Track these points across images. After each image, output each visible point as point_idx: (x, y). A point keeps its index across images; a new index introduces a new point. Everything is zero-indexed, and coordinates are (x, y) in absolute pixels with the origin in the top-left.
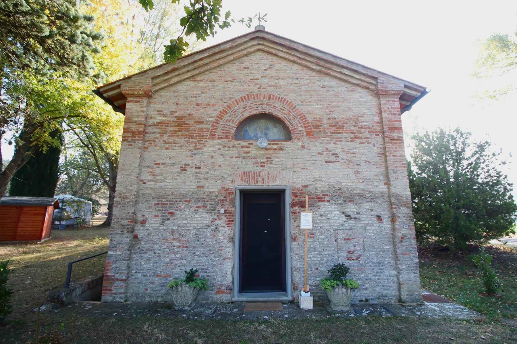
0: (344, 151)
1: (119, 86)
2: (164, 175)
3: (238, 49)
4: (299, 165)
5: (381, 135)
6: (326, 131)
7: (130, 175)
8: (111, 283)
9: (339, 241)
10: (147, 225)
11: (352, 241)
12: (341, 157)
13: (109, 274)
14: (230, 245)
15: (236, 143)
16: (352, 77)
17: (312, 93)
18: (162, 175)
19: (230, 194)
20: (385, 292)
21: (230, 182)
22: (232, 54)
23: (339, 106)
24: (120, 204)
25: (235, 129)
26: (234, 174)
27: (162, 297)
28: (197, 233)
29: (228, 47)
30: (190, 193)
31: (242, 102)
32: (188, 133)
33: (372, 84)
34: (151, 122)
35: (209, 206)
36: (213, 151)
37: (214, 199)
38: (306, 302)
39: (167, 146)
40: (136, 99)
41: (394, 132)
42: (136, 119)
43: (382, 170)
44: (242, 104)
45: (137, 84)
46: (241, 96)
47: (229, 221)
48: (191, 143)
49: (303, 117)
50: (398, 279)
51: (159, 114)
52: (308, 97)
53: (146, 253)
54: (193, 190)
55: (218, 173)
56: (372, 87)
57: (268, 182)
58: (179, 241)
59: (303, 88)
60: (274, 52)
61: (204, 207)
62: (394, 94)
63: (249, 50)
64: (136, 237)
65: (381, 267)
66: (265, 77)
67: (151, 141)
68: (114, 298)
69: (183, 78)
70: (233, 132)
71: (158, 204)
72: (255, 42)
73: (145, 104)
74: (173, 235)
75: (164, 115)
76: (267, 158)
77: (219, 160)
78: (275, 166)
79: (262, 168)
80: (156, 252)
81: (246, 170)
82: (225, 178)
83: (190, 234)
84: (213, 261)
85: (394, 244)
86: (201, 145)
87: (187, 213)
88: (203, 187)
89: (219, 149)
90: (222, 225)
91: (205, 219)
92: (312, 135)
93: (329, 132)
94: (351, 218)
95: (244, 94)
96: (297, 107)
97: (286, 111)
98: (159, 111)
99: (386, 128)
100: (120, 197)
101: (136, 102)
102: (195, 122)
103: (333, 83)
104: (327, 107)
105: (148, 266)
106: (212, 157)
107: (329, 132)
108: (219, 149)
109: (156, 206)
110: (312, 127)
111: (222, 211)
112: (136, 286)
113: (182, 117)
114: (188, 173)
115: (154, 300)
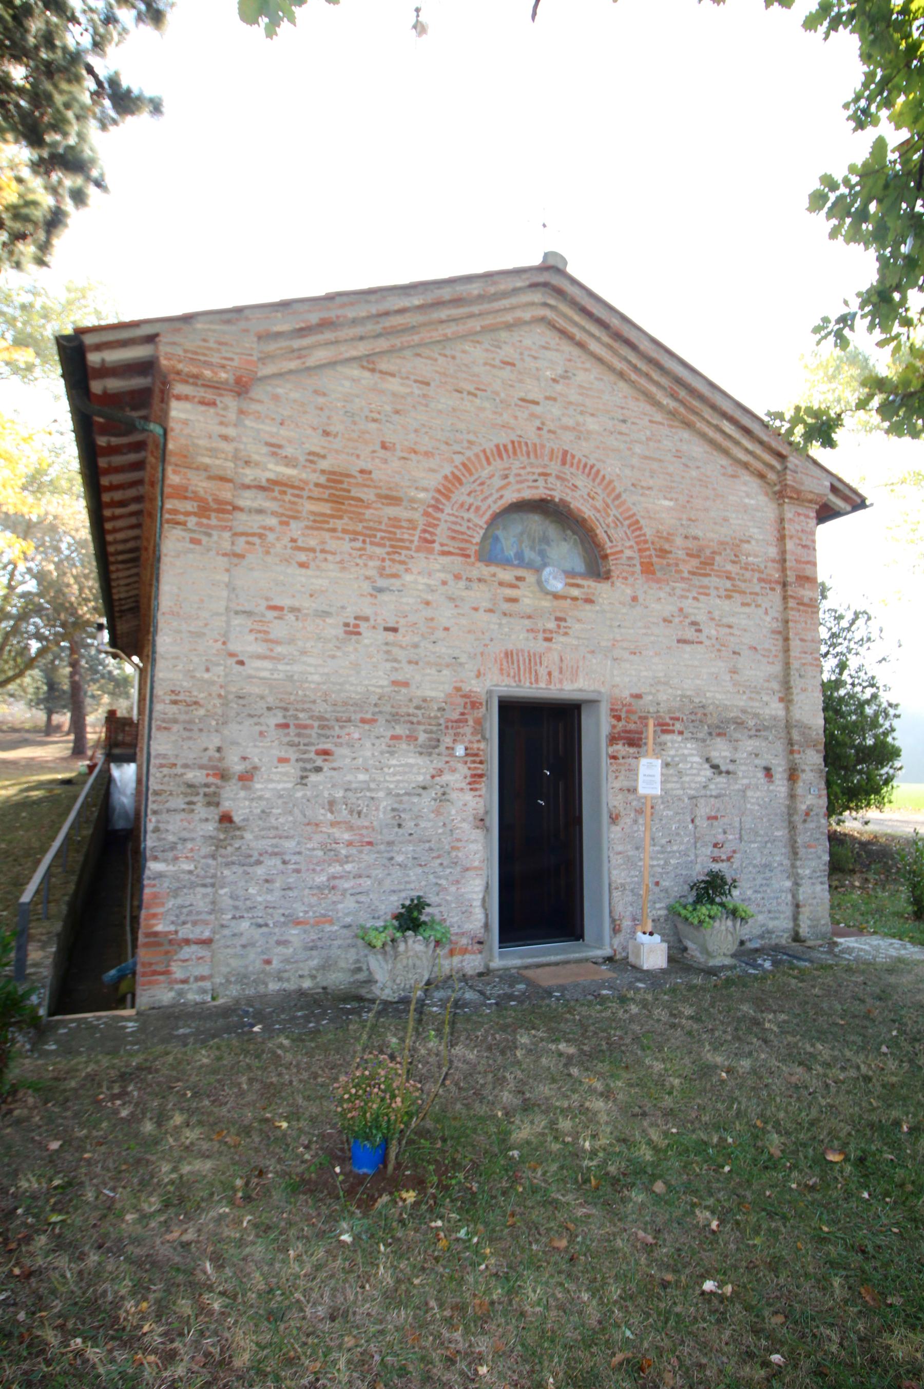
0: (712, 619)
1: (151, 339)
2: (300, 643)
3: (496, 305)
4: (625, 644)
5: (779, 589)
6: (681, 567)
7: (200, 635)
8: (167, 953)
9: (697, 822)
10: (258, 786)
11: (722, 821)
12: (706, 632)
13: (159, 928)
14: (478, 834)
15: (485, 570)
16: (737, 443)
17: (655, 465)
18: (292, 641)
19: (474, 705)
20: (771, 925)
21: (473, 674)
22: (480, 315)
23: (706, 510)
24: (175, 721)
25: (482, 532)
26: (482, 654)
27: (313, 977)
28: (396, 806)
29: (476, 292)
30: (374, 699)
31: (499, 461)
32: (359, 527)
33: (772, 467)
34: (249, 475)
35: (422, 737)
36: (428, 586)
37: (436, 717)
38: (653, 953)
39: (303, 557)
40: (201, 393)
41: (803, 586)
42: (207, 460)
43: (777, 668)
44: (498, 464)
45: (212, 344)
46: (496, 441)
47: (473, 776)
48: (371, 558)
49: (636, 525)
50: (794, 896)
51: (274, 454)
52: (647, 474)
53: (259, 863)
54: (379, 690)
55: (444, 650)
56: (772, 476)
57: (561, 681)
58: (351, 828)
59: (638, 449)
60: (579, 335)
61: (411, 738)
62: (811, 501)
63: (519, 314)
64: (226, 819)
65: (768, 874)
66: (555, 399)
67: (253, 535)
68: (181, 993)
69: (347, 355)
70: (477, 539)
71: (286, 726)
72: (537, 297)
73: (232, 416)
74: (332, 812)
75: (289, 462)
76: (558, 619)
77: (445, 614)
78: (575, 642)
79: (546, 644)
80: (287, 858)
81: (510, 647)
82: (461, 664)
83: (377, 809)
84: (439, 877)
85: (792, 827)
86: (398, 566)
87: (369, 754)
88: (406, 684)
89: (444, 583)
90: (458, 786)
91: (415, 770)
92: (653, 573)
93: (685, 568)
94: (720, 773)
95: (503, 438)
96: (624, 496)
97: (599, 504)
98: (272, 445)
99: (791, 578)
100: (175, 702)
101: (202, 403)
102: (379, 496)
103: (698, 449)
104: (684, 507)
105: (269, 898)
106: (428, 603)
107: (685, 568)
108: (444, 583)
109: (281, 732)
110: (653, 552)
111: (460, 751)
112: (235, 956)
113: (341, 474)
114: (366, 641)
115: (291, 986)
